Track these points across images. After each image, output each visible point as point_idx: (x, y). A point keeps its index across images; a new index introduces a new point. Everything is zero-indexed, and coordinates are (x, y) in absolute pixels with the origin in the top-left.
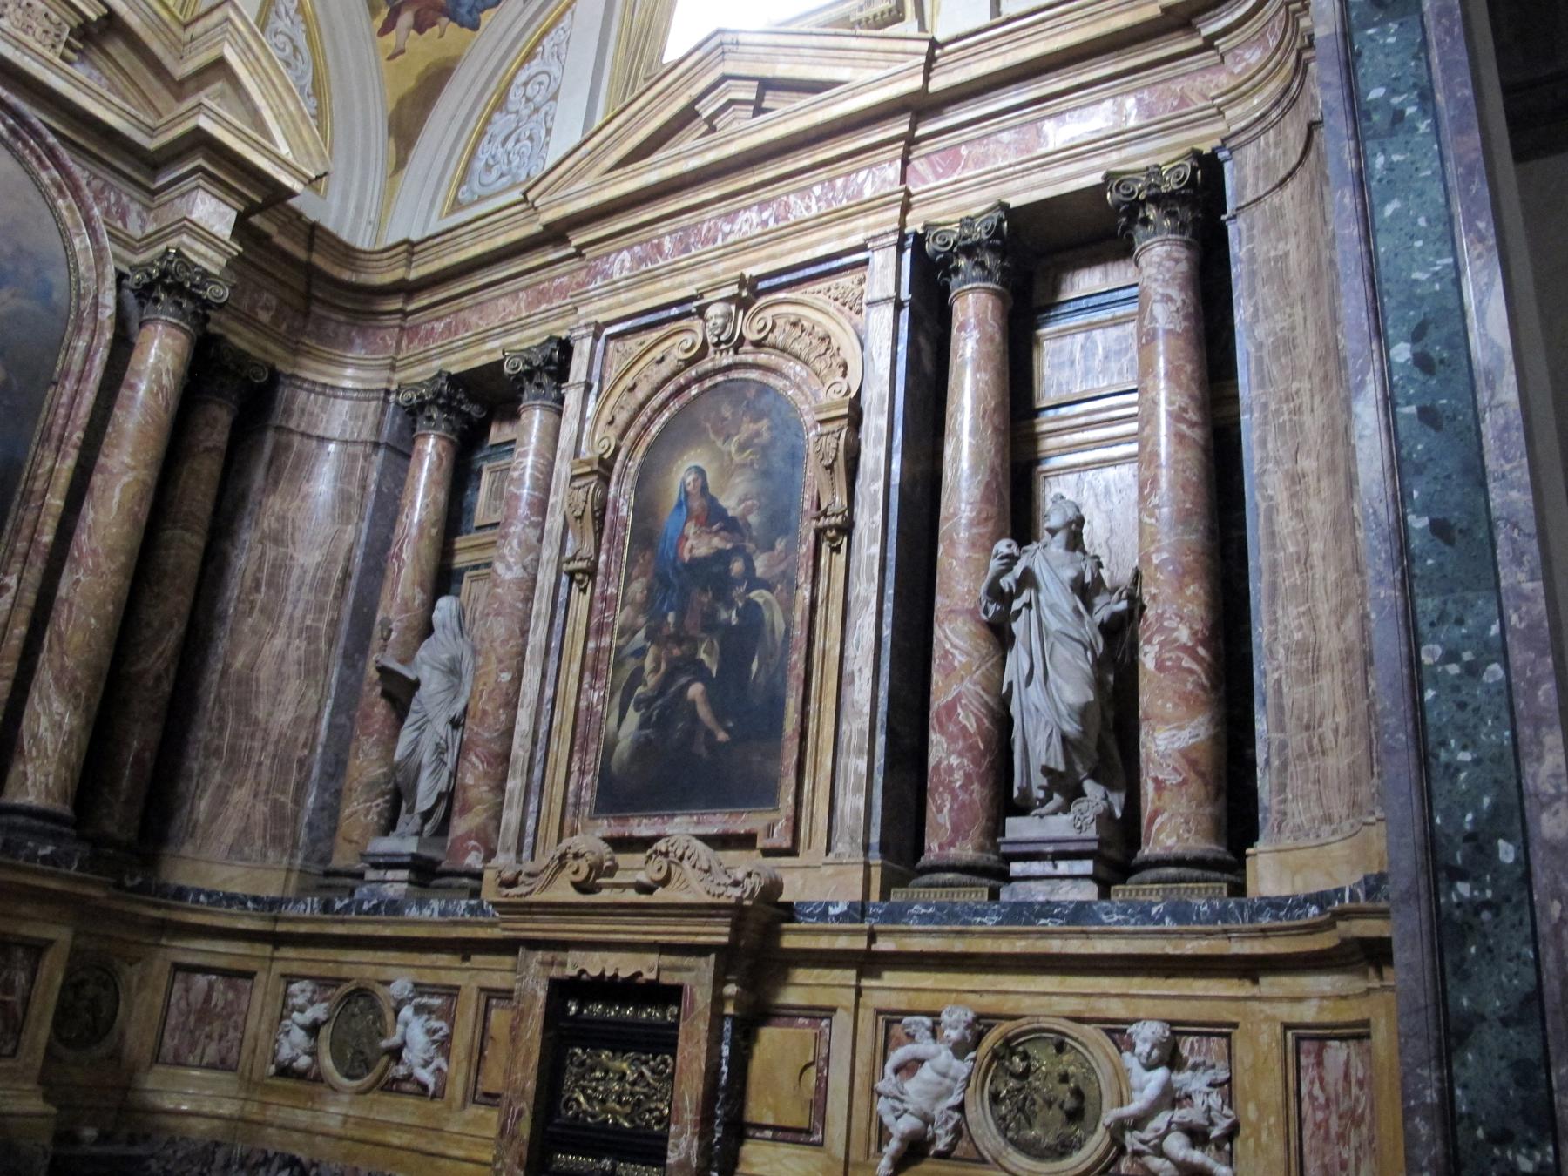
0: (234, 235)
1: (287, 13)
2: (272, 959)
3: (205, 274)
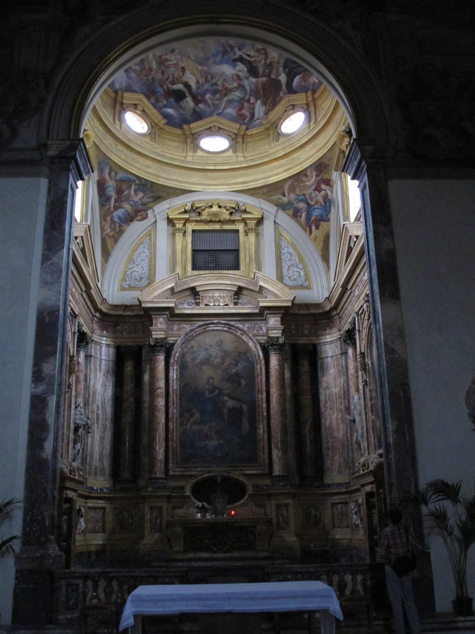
0: (282, 324)
1: (285, 247)
2: (350, 498)
3: (278, 338)
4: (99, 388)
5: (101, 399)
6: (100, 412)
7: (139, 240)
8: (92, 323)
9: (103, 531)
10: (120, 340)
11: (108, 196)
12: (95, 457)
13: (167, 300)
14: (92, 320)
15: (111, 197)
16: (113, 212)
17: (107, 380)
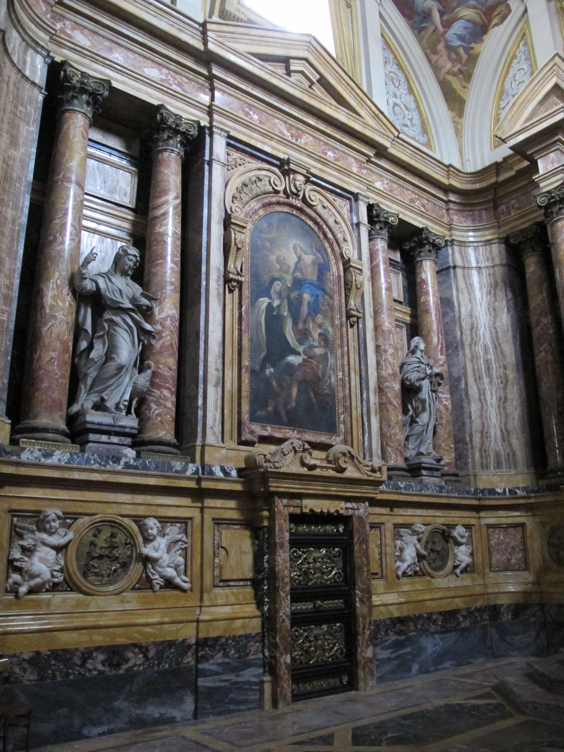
4: (483, 318)
5: (491, 333)
6: (491, 356)
7: (508, 55)
8: (448, 214)
9: (526, 568)
10: (511, 225)
11: (424, 12)
12: (492, 435)
13: (547, 113)
14: (448, 210)
15: (430, 10)
16: (445, 33)
17: (496, 300)
